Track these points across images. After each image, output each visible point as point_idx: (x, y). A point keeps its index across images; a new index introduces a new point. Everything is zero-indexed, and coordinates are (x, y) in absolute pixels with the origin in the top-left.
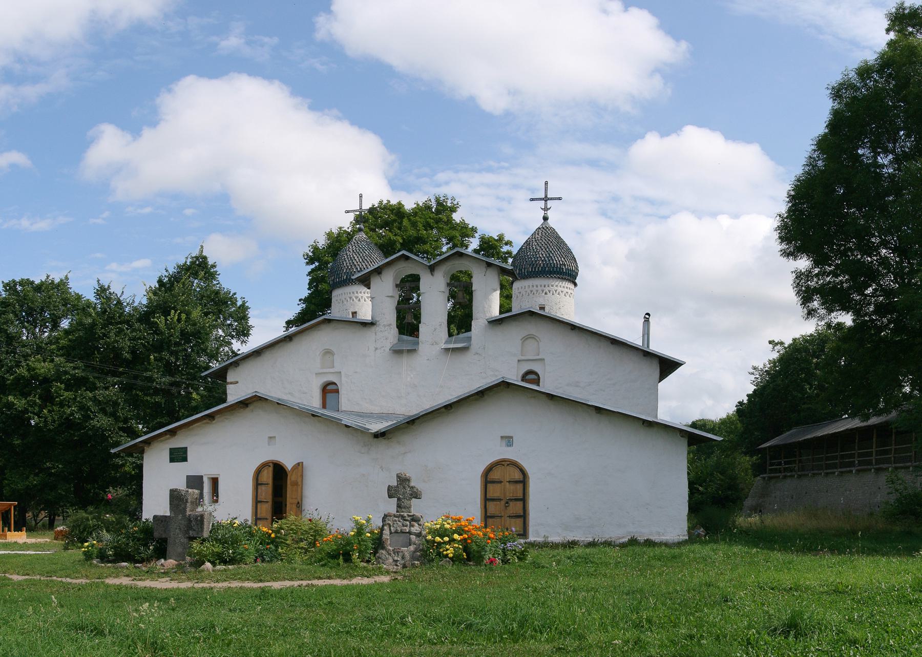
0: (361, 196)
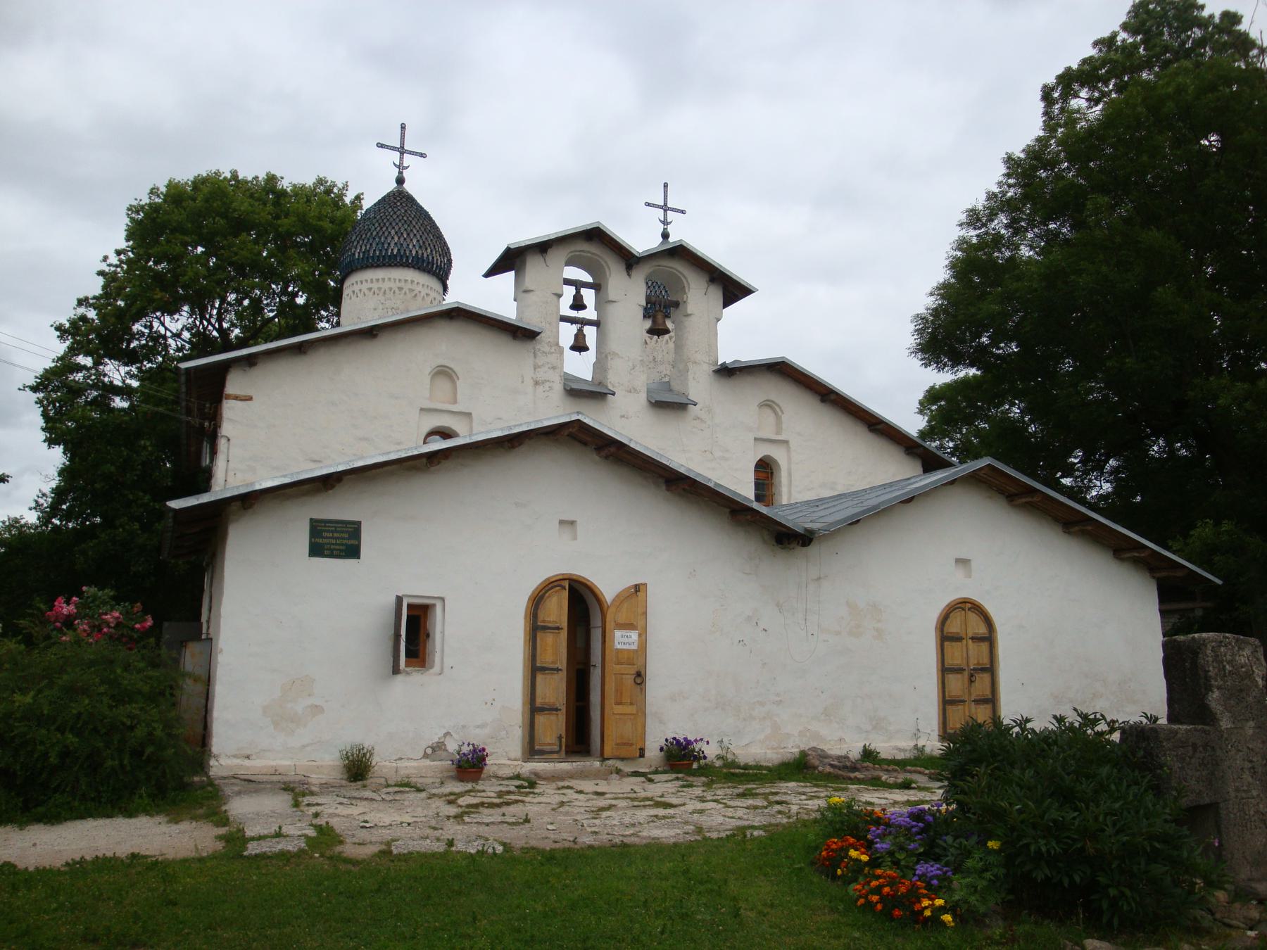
0: (403, 127)
